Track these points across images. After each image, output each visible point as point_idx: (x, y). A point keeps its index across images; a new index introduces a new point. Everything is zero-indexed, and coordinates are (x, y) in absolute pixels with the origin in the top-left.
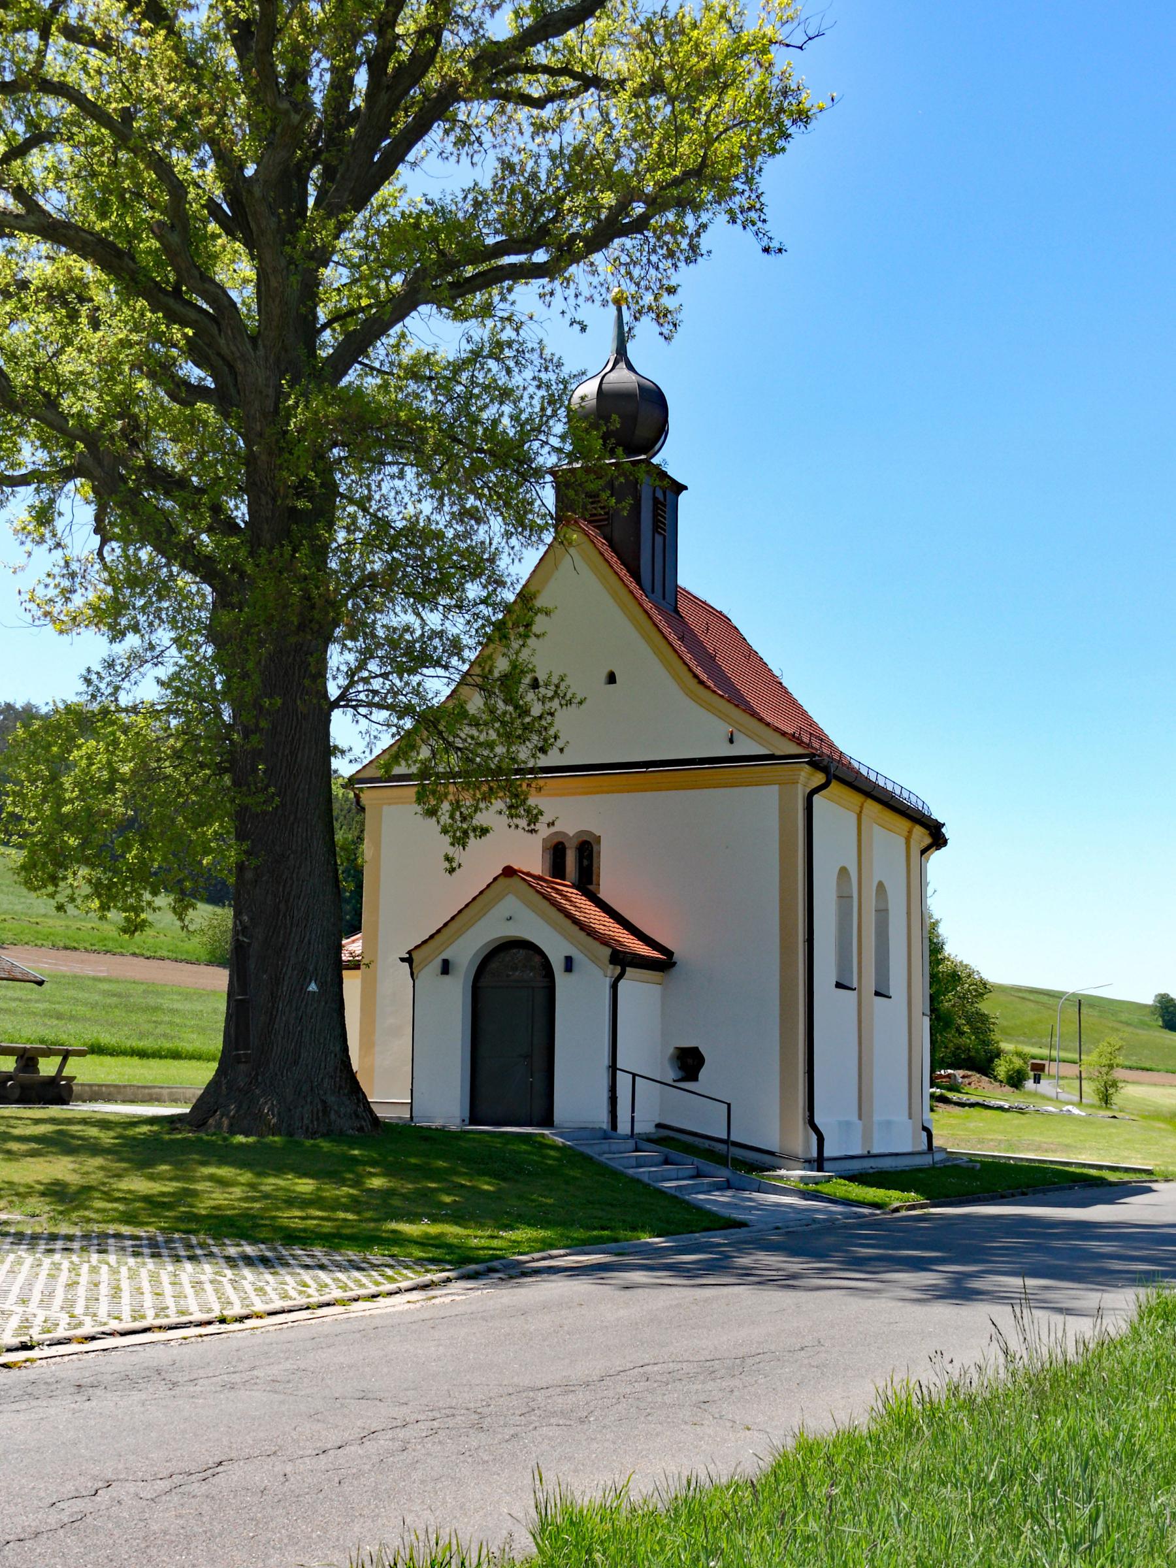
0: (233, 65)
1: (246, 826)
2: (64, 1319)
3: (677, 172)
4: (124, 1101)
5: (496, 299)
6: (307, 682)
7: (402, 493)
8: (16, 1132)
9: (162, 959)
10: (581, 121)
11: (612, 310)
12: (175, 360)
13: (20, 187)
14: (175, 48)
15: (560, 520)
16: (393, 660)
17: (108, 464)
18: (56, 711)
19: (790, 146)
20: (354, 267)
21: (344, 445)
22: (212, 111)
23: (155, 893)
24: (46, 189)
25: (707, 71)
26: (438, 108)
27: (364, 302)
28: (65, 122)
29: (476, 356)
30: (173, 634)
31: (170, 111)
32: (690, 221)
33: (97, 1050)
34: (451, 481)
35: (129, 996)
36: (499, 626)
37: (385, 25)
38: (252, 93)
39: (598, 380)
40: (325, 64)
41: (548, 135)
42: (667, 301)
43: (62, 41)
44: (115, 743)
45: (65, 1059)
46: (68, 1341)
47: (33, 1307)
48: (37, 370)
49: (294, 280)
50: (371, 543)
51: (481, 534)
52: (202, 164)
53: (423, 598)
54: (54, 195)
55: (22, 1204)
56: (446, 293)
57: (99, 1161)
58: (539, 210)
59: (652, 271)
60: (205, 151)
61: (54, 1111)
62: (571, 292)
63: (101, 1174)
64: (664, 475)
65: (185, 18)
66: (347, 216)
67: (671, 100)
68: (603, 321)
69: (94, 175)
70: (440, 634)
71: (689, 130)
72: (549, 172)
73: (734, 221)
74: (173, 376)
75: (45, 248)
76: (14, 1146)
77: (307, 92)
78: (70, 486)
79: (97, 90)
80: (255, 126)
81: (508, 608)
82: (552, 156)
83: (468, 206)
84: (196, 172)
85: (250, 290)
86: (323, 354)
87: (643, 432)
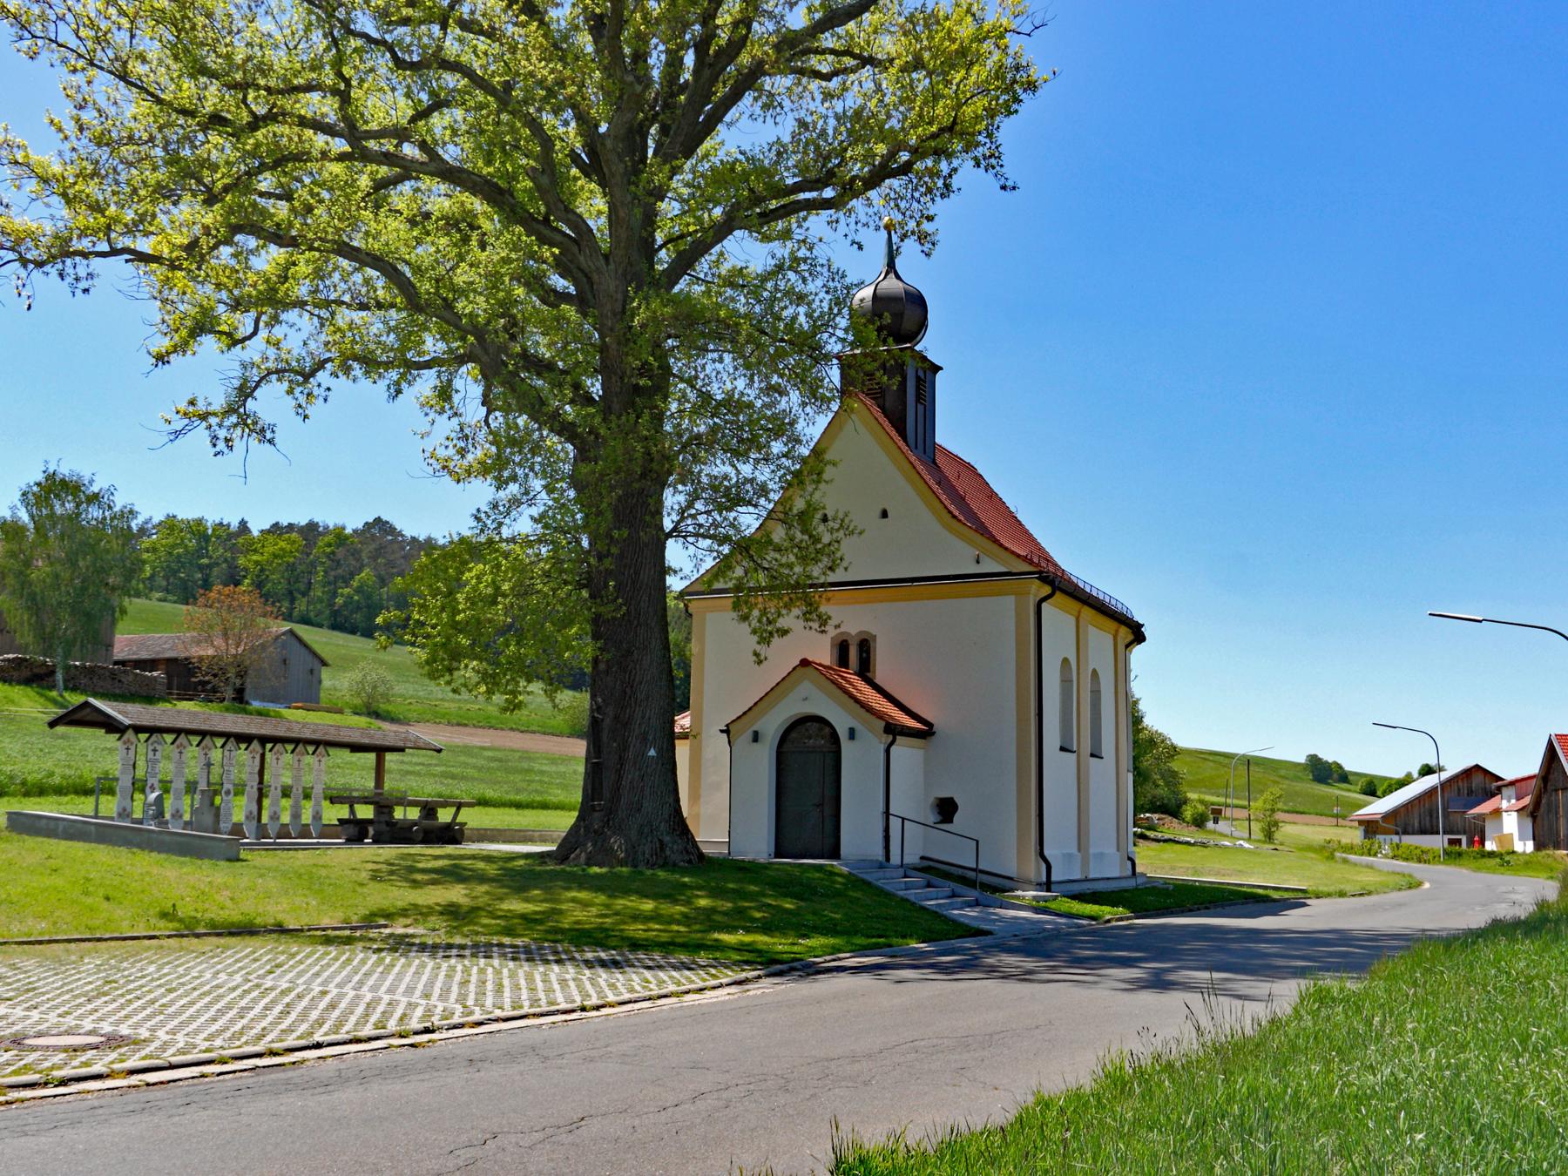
0: (590, 49)
1: (599, 628)
2: (459, 1009)
3: (934, 129)
4: (504, 842)
5: (794, 226)
6: (648, 518)
7: (722, 374)
8: (420, 865)
9: (534, 732)
10: (859, 89)
11: (884, 234)
12: (544, 272)
13: (424, 141)
14: (545, 36)
15: (844, 392)
16: (715, 501)
17: (494, 354)
18: (451, 542)
19: (1022, 108)
20: (683, 201)
21: (676, 337)
22: (573, 83)
23: (529, 681)
24: (445, 144)
25: (957, 51)
26: (749, 80)
27: (691, 229)
28: (459, 91)
29: (780, 268)
30: (543, 482)
31: (541, 83)
32: (944, 166)
33: (483, 802)
34: (759, 363)
35: (507, 761)
36: (796, 474)
37: (708, 18)
38: (605, 69)
39: (872, 288)
40: (661, 47)
41: (835, 101)
42: (927, 227)
43: (458, 31)
44: (498, 566)
45: (458, 809)
46: (462, 1026)
47: (434, 1000)
48: (437, 281)
49: (638, 212)
50: (696, 411)
51: (783, 404)
52: (566, 123)
53: (738, 455)
54: (451, 147)
55: (425, 921)
56: (755, 221)
57: (484, 888)
58: (827, 158)
59: (915, 205)
60: (568, 114)
61: (450, 849)
62: (852, 220)
63: (486, 898)
64: (925, 359)
65: (553, 13)
66: (678, 163)
67: (930, 74)
68: (876, 243)
69: (482, 132)
70: (752, 481)
71: (943, 97)
72: (835, 129)
73: (978, 165)
74: (542, 286)
75: (443, 188)
76: (419, 877)
77: (648, 68)
78: (464, 369)
79: (484, 67)
80: (607, 94)
81: (804, 461)
82: (837, 117)
83: (773, 154)
84: (561, 130)
85: (603, 219)
86: (659, 267)
87: (908, 325)
